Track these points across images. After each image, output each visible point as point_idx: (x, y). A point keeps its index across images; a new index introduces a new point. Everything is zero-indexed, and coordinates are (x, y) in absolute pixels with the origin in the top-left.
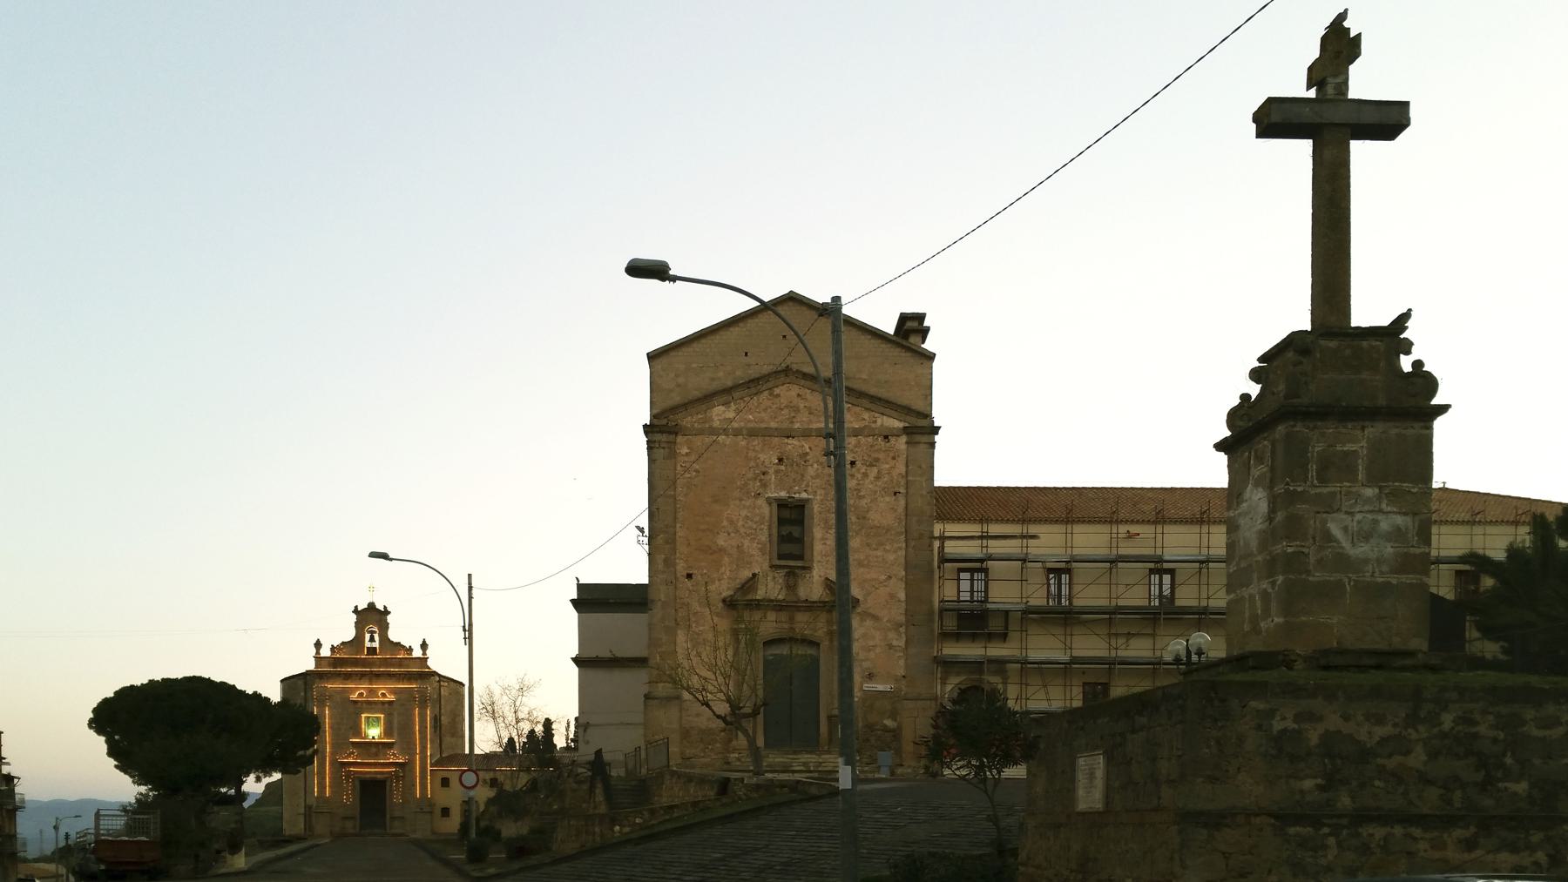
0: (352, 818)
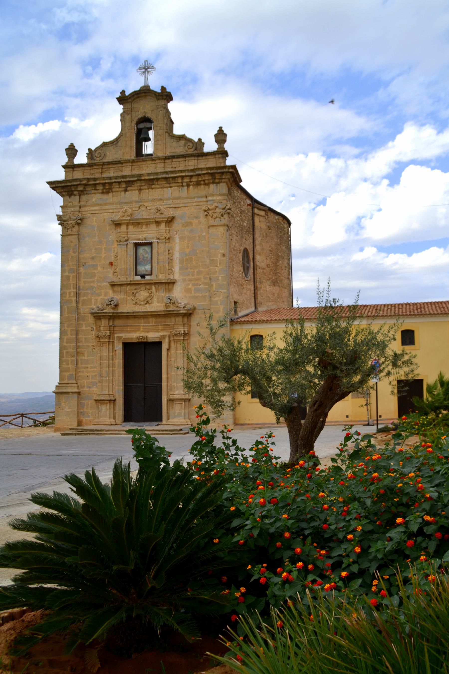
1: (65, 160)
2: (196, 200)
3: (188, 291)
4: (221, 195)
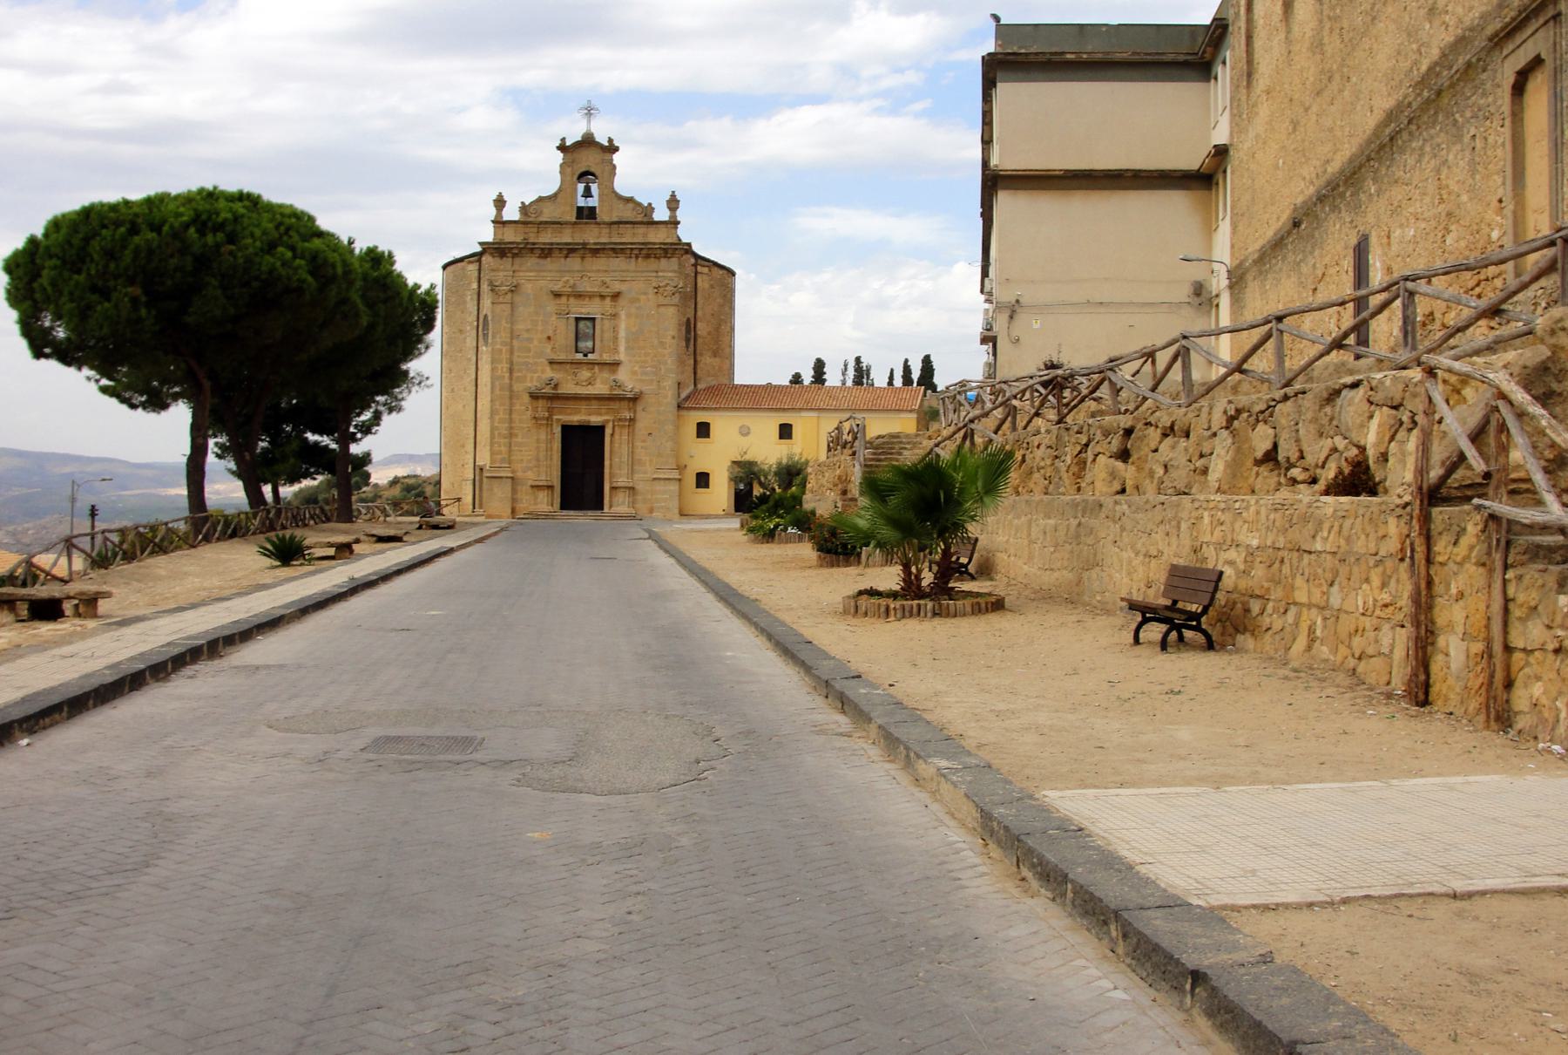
0: (551, 487)
1: (493, 212)
2: (644, 275)
3: (634, 373)
4: (671, 271)
